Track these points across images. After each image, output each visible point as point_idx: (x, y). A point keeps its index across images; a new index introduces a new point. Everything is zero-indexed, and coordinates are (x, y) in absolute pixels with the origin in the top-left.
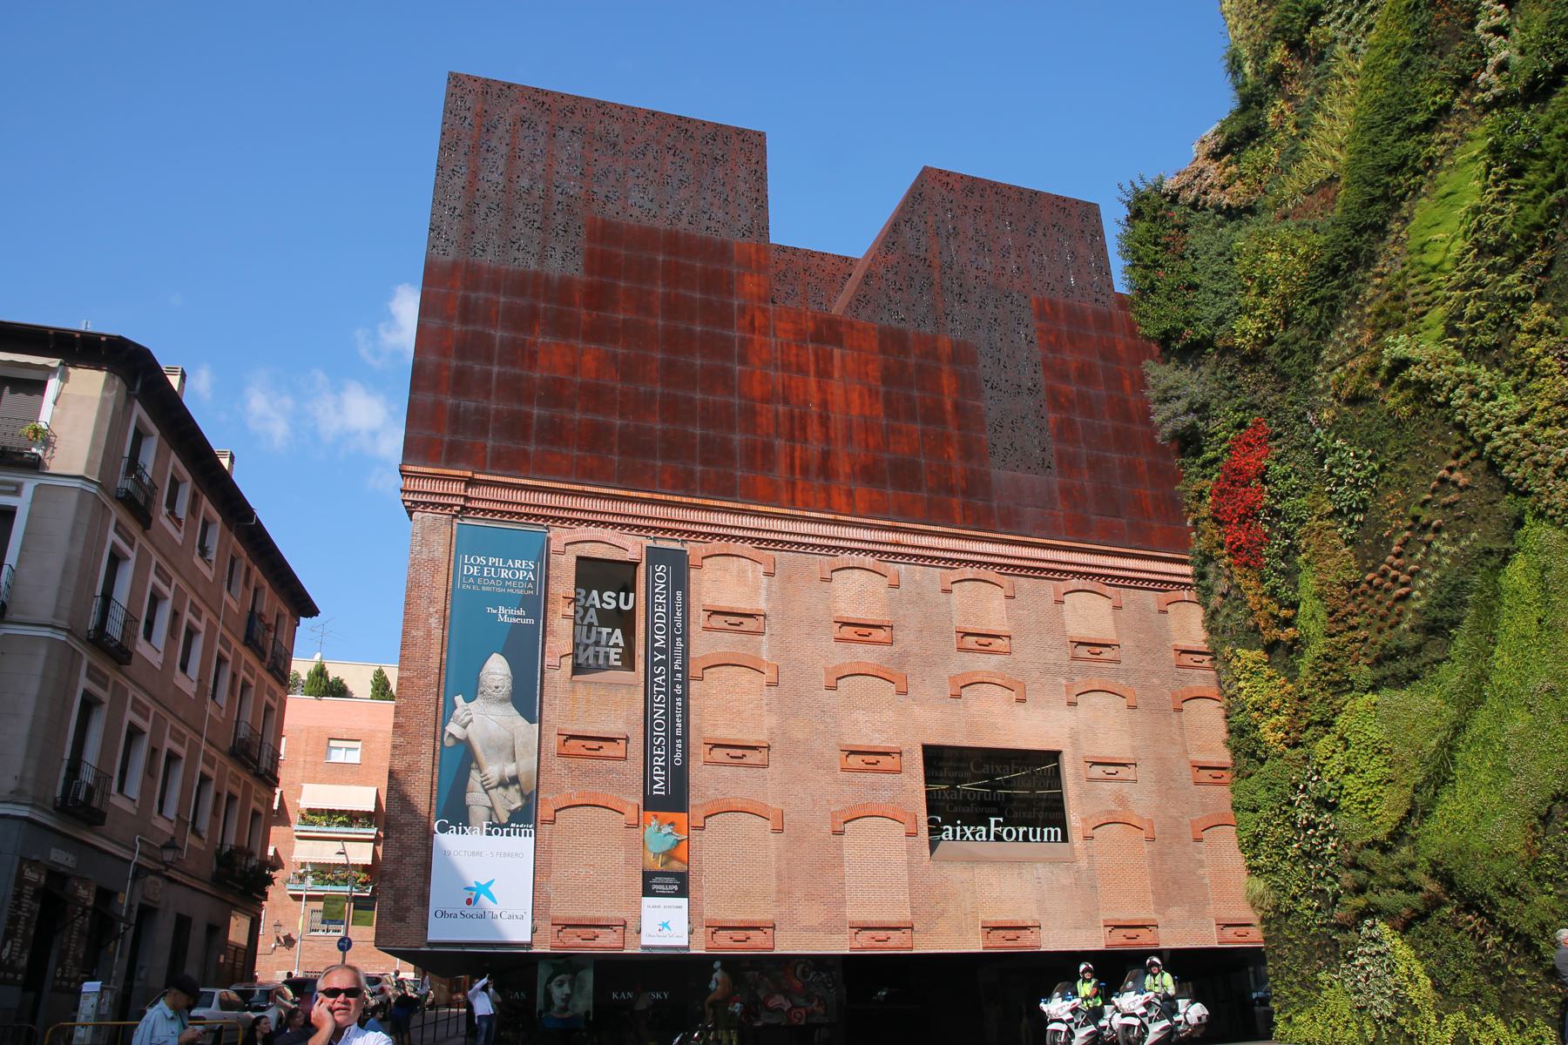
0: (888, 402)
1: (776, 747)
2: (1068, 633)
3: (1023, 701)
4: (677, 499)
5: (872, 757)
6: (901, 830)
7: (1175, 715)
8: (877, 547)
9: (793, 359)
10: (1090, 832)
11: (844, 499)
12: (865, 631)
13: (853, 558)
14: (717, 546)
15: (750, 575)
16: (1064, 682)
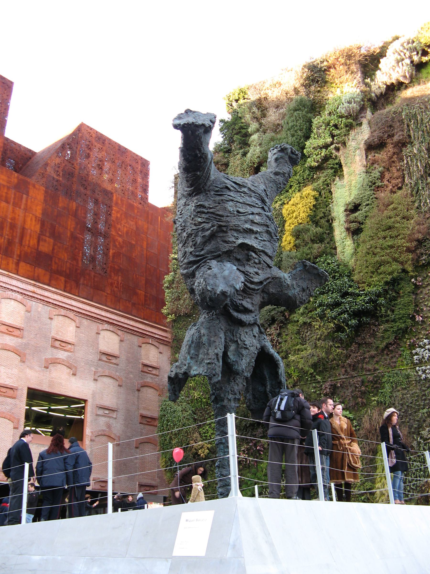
0: (43, 224)
2: (100, 348)
3: (74, 374)
6: (11, 425)
7: (137, 392)
8: (24, 292)
9: (4, 194)
10: (93, 438)
11: (14, 266)
12: (11, 329)
13: (12, 295)
16: (94, 370)
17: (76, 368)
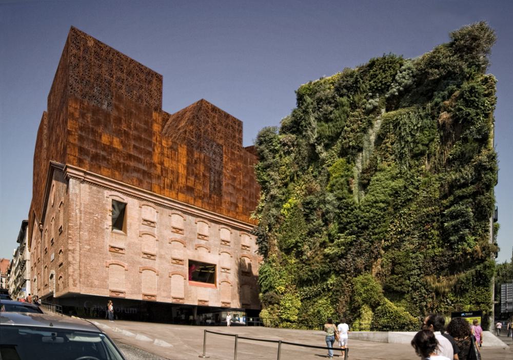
0: (188, 170)
1: (158, 256)
3: (209, 252)
4: (137, 188)
5: (178, 261)
14: (145, 202)
15: (153, 211)
17: (210, 248)
